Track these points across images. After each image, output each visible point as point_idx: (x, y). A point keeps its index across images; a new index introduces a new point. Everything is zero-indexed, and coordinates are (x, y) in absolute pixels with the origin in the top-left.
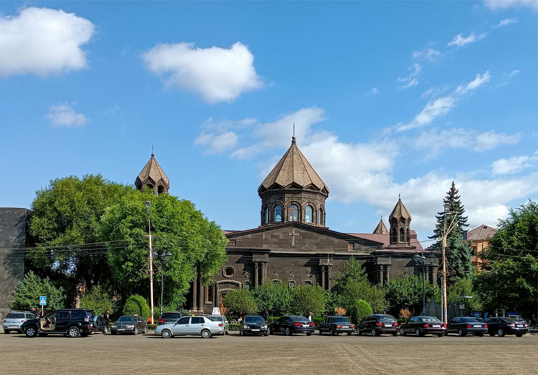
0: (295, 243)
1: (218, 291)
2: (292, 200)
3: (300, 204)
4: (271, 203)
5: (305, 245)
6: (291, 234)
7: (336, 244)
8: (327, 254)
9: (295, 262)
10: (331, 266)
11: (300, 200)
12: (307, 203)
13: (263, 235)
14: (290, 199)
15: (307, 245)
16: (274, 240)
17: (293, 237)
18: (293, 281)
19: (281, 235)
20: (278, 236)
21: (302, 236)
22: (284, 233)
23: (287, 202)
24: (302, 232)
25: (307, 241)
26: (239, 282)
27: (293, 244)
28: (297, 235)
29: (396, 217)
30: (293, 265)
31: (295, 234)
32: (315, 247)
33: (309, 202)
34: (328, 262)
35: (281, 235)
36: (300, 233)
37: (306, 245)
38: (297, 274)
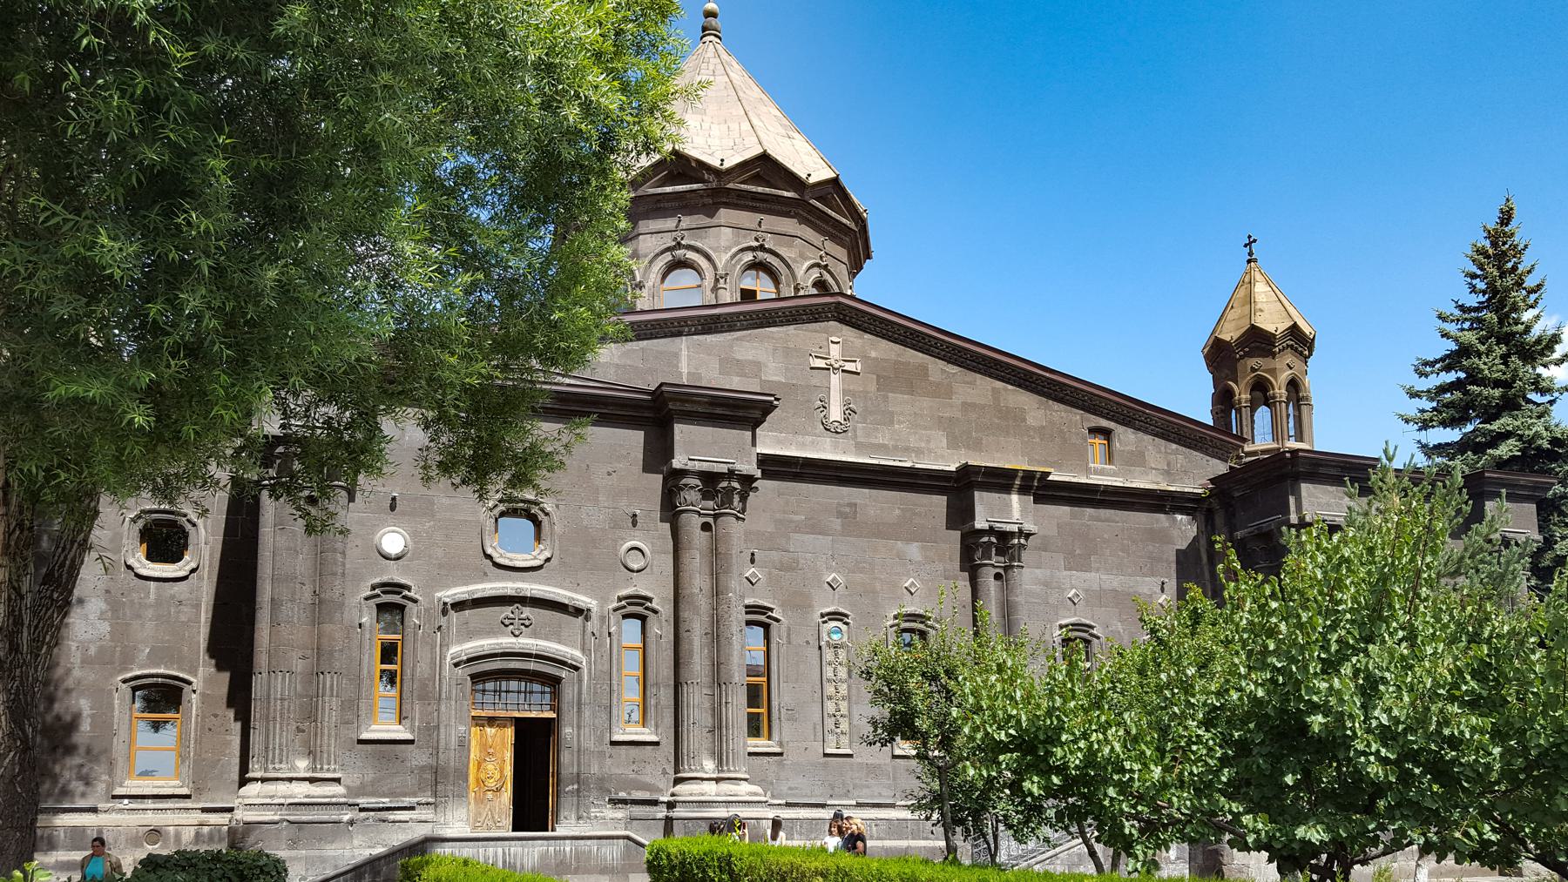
0: (849, 412)
1: (454, 649)
2: (756, 244)
3: (789, 266)
4: (646, 256)
5: (892, 422)
6: (821, 363)
7: (1034, 428)
8: (1009, 474)
9: (848, 510)
10: (1028, 536)
11: (790, 246)
12: (812, 266)
13: (676, 355)
14: (745, 237)
15: (900, 422)
17: (835, 380)
18: (841, 610)
19: (772, 365)
20: (758, 365)
21: (875, 377)
22: (787, 352)
23: (734, 250)
24: (873, 354)
25: (899, 402)
26: (589, 600)
27: (836, 413)
28: (850, 367)
29: (1270, 328)
30: (837, 524)
31: (841, 363)
32: (940, 440)
33: (818, 265)
34: (1014, 511)
35: (772, 365)
37: (897, 426)
38: (859, 577)
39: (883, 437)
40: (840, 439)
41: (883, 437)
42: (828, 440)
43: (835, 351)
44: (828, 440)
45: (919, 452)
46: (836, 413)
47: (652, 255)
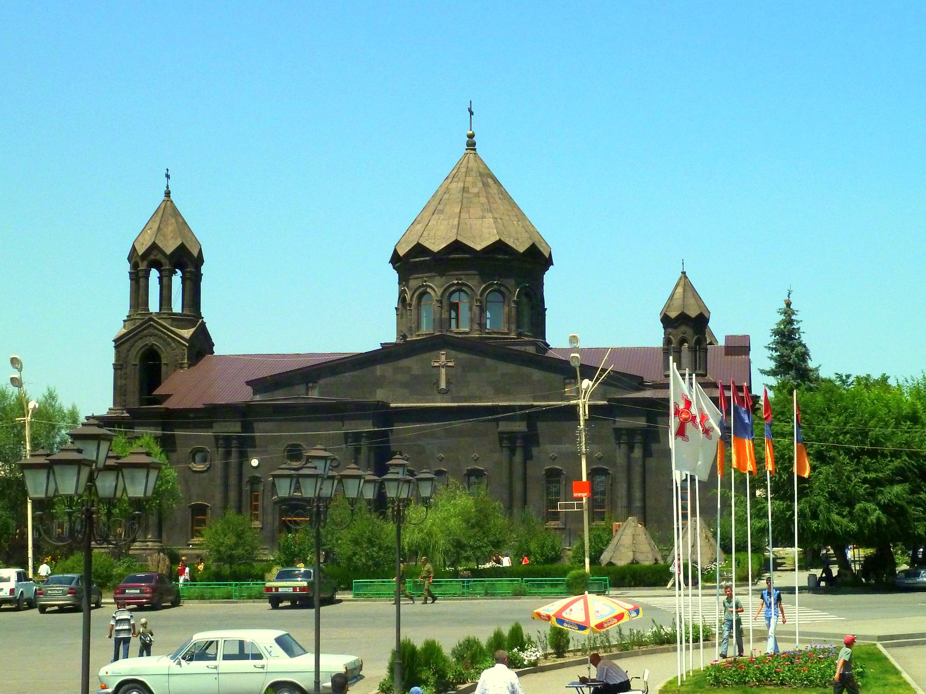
0: (448, 382)
2: (456, 282)
6: (436, 364)
16: (400, 377)
17: (443, 371)
20: (409, 368)
27: (443, 385)
36: (456, 359)
37: (470, 387)
39: (464, 393)
40: (445, 396)
41: (464, 393)
42: (439, 396)
43: (443, 358)
44: (439, 397)
45: (480, 400)
46: (443, 385)
47: (414, 289)
